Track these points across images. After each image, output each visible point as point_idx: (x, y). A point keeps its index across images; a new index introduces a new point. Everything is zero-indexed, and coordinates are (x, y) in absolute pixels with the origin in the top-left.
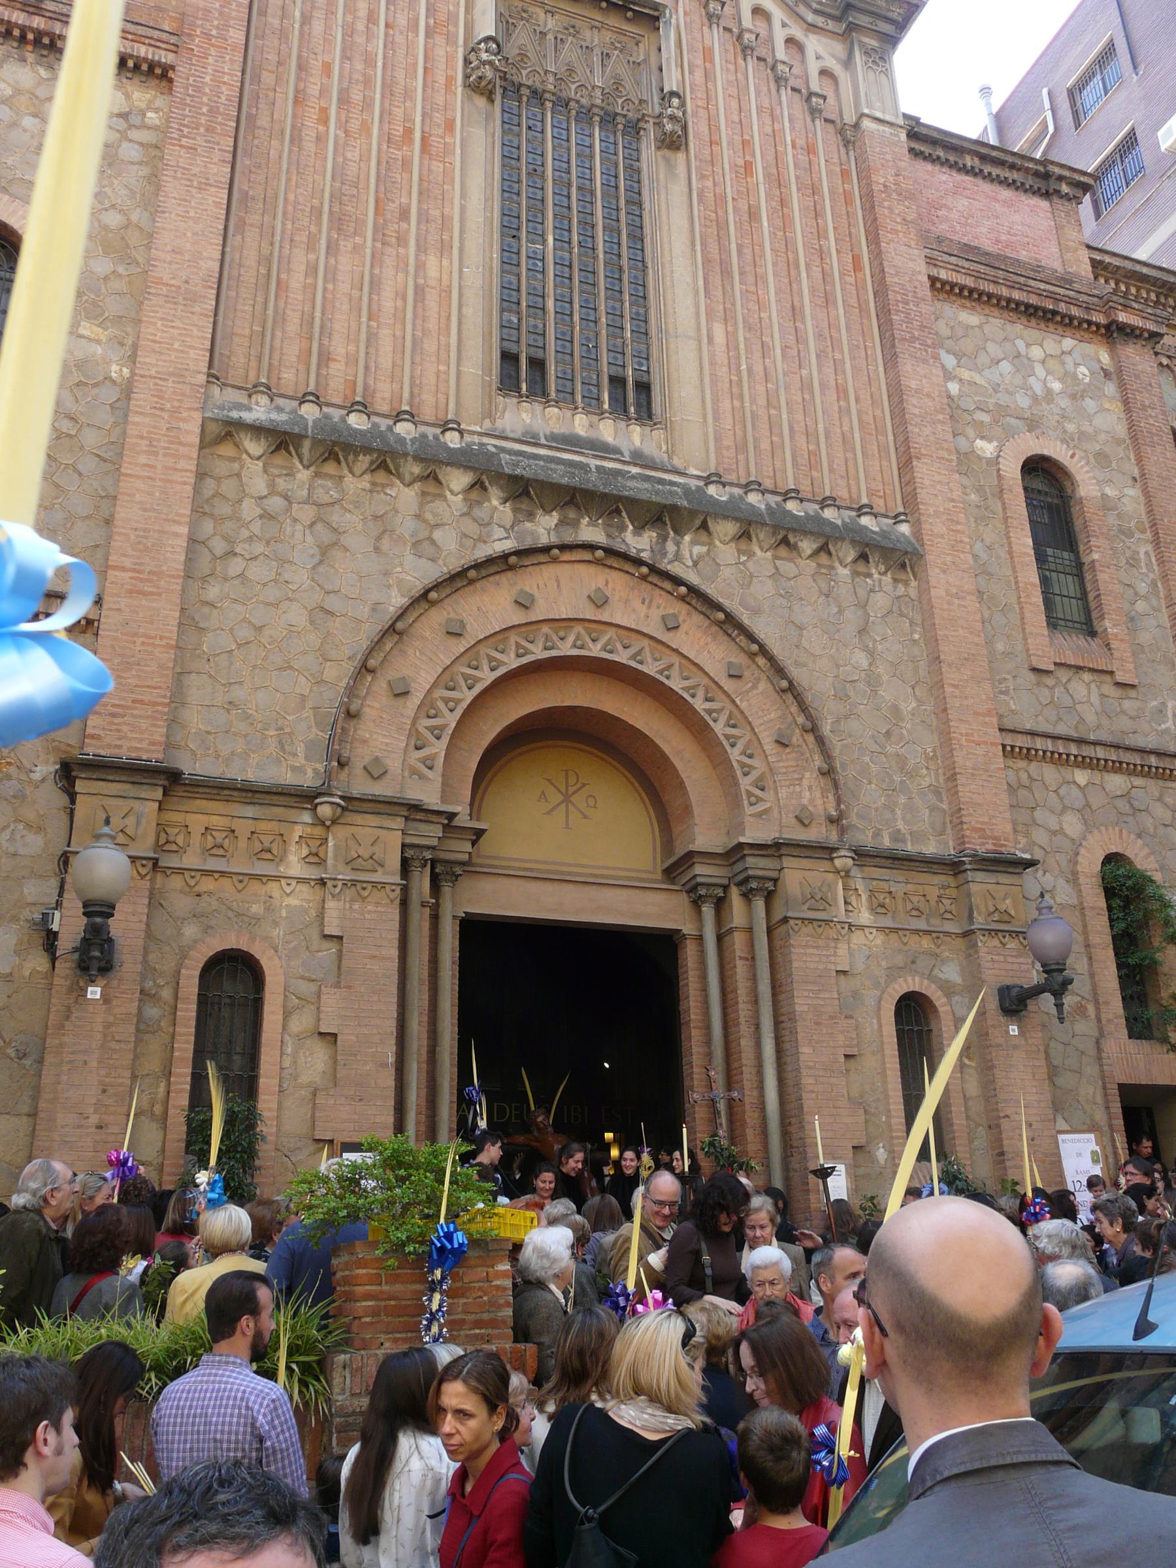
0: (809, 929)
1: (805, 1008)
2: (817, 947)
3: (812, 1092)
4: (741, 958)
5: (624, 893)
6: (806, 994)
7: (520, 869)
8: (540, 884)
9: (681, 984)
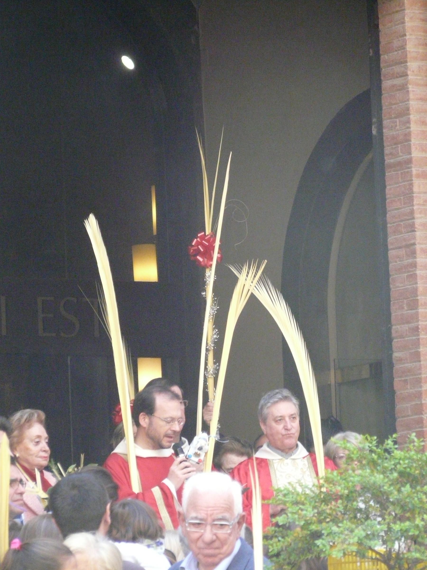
9: (386, 84)
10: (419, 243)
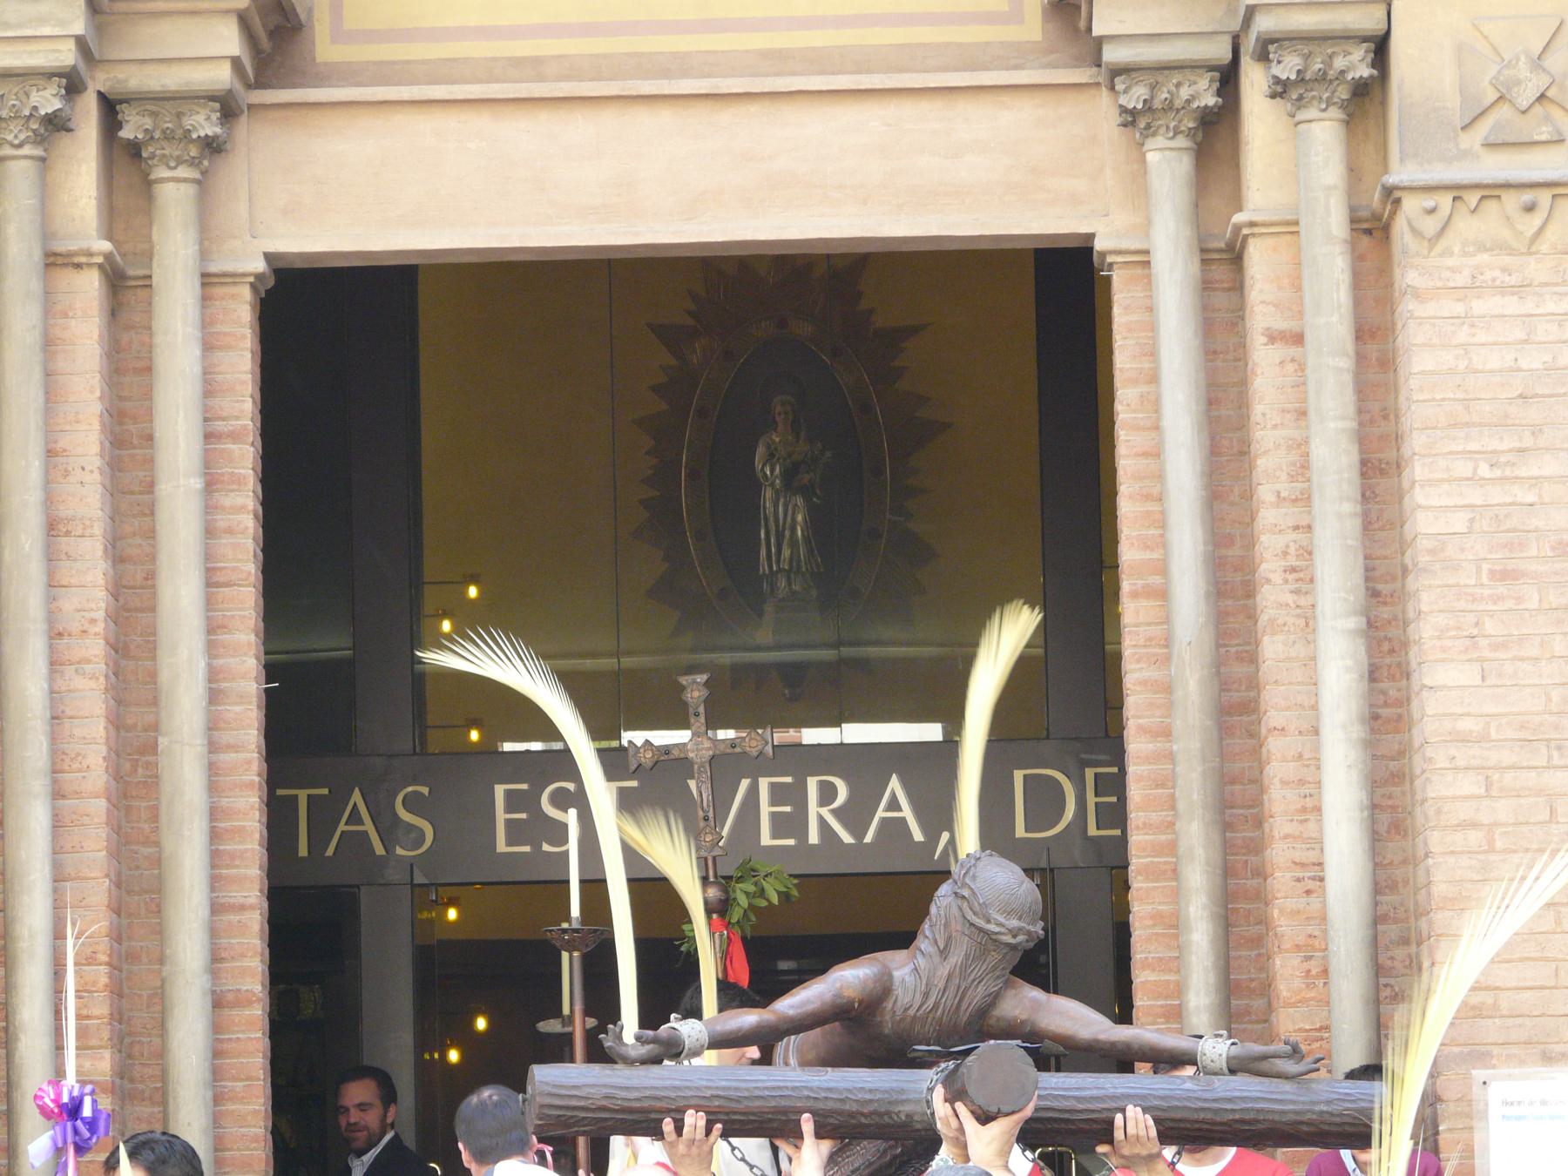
0: (1489, 222)
1: (1459, 522)
2: (1520, 290)
3: (1474, 825)
4: (1273, 337)
5: (872, 119)
6: (1463, 468)
7: (490, 70)
8: (544, 120)
10: (1135, 717)
